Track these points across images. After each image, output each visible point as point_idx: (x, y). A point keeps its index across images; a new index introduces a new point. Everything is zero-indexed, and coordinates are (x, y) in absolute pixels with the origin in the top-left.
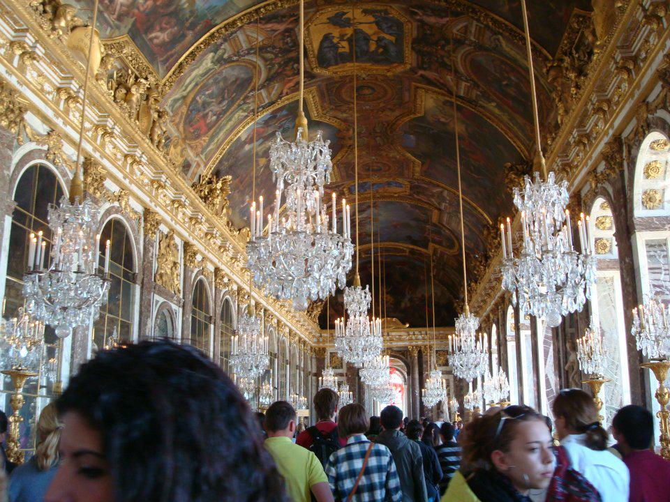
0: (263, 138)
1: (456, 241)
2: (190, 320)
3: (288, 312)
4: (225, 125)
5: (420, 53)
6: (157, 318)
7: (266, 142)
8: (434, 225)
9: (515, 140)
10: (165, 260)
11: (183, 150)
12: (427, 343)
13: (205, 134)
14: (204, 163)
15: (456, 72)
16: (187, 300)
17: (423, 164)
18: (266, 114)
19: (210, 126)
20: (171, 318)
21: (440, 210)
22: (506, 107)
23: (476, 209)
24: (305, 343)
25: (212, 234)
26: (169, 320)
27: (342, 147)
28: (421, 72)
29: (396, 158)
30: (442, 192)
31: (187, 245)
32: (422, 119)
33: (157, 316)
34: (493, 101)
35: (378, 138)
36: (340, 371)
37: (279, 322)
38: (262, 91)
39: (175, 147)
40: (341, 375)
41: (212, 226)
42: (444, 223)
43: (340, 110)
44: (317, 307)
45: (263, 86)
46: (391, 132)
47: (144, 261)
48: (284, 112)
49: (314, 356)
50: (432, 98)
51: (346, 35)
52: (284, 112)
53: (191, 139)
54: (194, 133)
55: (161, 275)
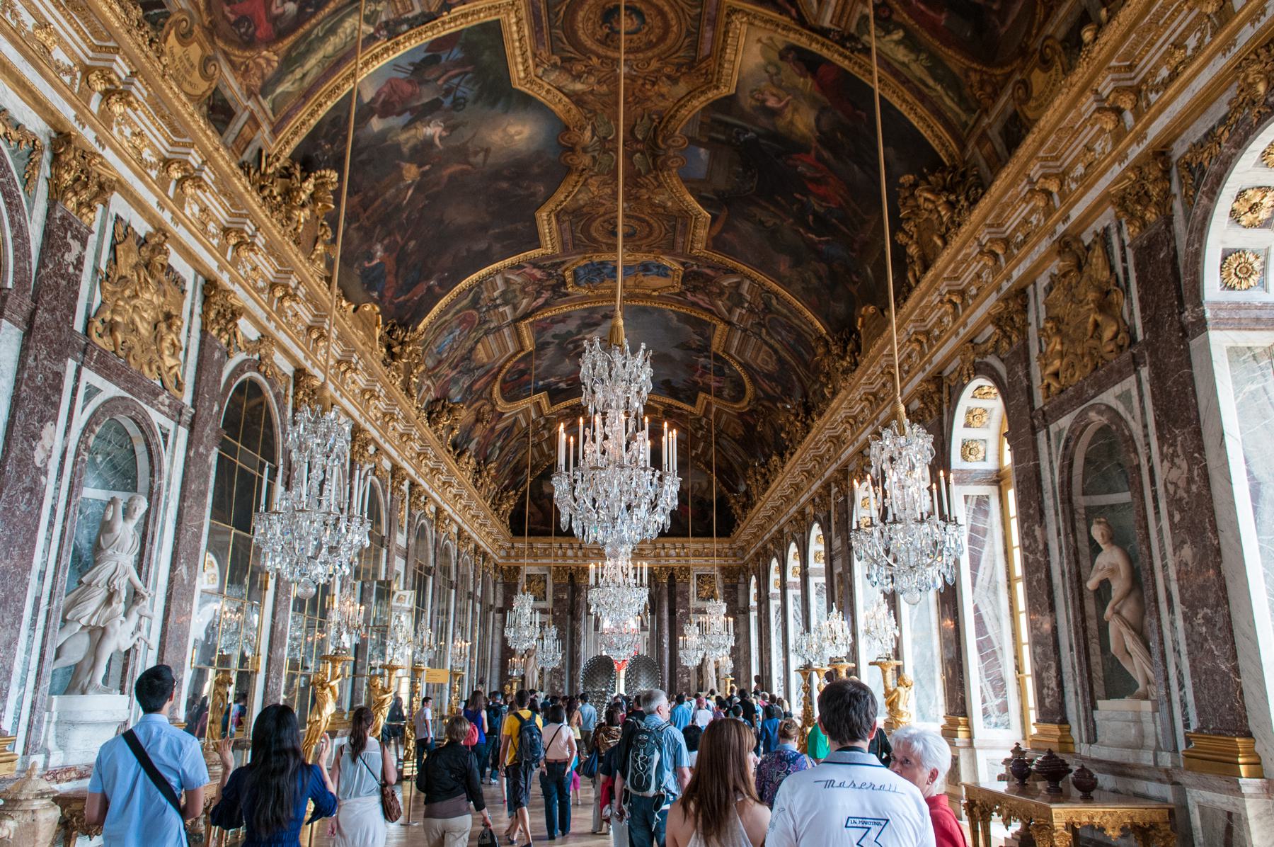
0: (412, 110)
1: (748, 386)
2: (213, 459)
4: (322, 40)
6: (88, 428)
7: (418, 124)
8: (717, 357)
9: (933, 121)
10: (127, 293)
11: (206, 61)
12: (683, 563)
13: (269, 43)
14: (271, 123)
16: (204, 413)
17: (714, 219)
18: (412, 44)
19: (281, 26)
20: (148, 445)
21: (729, 323)
22: (925, 36)
24: (485, 554)
25: (286, 286)
26: (140, 449)
29: (665, 208)
30: (739, 285)
31: (210, 287)
32: (727, 104)
33: (88, 424)
34: (899, 26)
35: (638, 155)
36: (542, 605)
37: (439, 510)
39: (184, 38)
40: (543, 611)
41: (286, 268)
42: (733, 352)
43: (569, 71)
44: (508, 498)
46: (664, 141)
47: (42, 264)
48: (457, 54)
49: (500, 580)
50: (759, 41)
52: (457, 54)
53: (229, 41)
54: (237, 24)
55: (111, 328)
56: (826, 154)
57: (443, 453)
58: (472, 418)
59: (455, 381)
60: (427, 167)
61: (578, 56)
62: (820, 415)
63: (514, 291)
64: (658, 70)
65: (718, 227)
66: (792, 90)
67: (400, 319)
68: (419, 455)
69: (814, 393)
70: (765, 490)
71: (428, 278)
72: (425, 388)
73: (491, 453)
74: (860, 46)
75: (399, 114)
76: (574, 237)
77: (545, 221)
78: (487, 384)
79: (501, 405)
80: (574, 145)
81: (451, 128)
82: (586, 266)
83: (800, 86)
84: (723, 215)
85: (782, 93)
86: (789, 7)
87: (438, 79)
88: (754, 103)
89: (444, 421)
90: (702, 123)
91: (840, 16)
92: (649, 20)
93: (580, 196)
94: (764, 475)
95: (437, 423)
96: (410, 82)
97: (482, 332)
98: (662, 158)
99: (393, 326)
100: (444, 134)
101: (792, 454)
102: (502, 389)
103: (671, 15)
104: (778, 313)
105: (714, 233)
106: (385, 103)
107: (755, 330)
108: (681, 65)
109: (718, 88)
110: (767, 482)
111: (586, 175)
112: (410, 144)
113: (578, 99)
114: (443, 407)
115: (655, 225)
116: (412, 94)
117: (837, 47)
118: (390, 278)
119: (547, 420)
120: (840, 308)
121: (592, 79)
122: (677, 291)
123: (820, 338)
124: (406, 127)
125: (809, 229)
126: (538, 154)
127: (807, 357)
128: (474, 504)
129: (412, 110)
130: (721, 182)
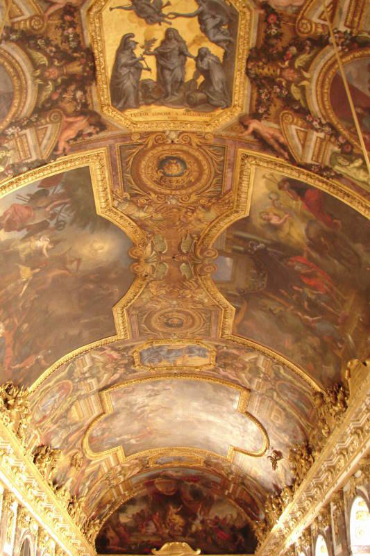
0: (29, 228)
3: (56, 520)
5: (257, 82)
7: (32, 238)
15: (304, 112)
17: (238, 311)
18: (30, 181)
23: (301, 377)
27: (136, 276)
28: (254, 125)
29: (202, 303)
30: (256, 359)
32: (244, 224)
35: (184, 264)
37: (40, 530)
38: (27, 131)
43: (136, 204)
44: (94, 525)
45: (30, 124)
46: (202, 252)
48: (59, 189)
50: (264, 177)
51: (154, 40)
52: (59, 189)
56: (314, 255)
57: (44, 485)
58: (68, 462)
59: (55, 433)
60: (37, 270)
61: (141, 192)
62: (320, 450)
63: (98, 367)
64: (196, 202)
65: (241, 316)
66: (289, 210)
67: (15, 381)
68: (26, 484)
69: (313, 438)
70: (279, 515)
71: (36, 353)
72: (33, 436)
73: (82, 490)
74: (333, 174)
75: (19, 230)
76: (139, 327)
77: (119, 317)
78: (80, 437)
79: (89, 454)
80: (139, 257)
81: (55, 242)
82: (148, 349)
83: (294, 206)
84: (244, 308)
85: (281, 213)
86: (282, 151)
87: (46, 207)
88: (263, 222)
89: (47, 461)
90: (227, 239)
91: (317, 156)
92: (189, 166)
93: (143, 296)
94: (278, 505)
95: (41, 463)
96: (27, 207)
97: (75, 397)
98: (200, 266)
99: (10, 386)
100: (50, 247)
101: (299, 485)
102: (90, 442)
103: (204, 162)
104: (285, 379)
105: (238, 322)
106: (9, 222)
107: (270, 394)
108: (211, 197)
109: (237, 212)
110: (281, 510)
111: (148, 279)
112: (27, 251)
113: (142, 225)
114: (46, 451)
115: (196, 317)
116: (29, 216)
117: (317, 176)
118: (9, 350)
119: (123, 468)
120: (330, 370)
121: (151, 209)
122: (212, 367)
123: (316, 393)
124: (24, 239)
125: (305, 312)
126: (115, 264)
127: (307, 410)
128: (68, 527)
129: (29, 228)
130: (242, 283)
